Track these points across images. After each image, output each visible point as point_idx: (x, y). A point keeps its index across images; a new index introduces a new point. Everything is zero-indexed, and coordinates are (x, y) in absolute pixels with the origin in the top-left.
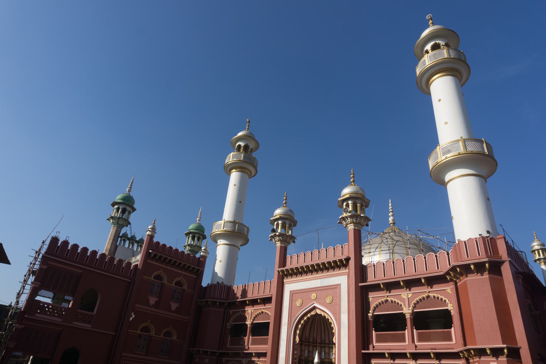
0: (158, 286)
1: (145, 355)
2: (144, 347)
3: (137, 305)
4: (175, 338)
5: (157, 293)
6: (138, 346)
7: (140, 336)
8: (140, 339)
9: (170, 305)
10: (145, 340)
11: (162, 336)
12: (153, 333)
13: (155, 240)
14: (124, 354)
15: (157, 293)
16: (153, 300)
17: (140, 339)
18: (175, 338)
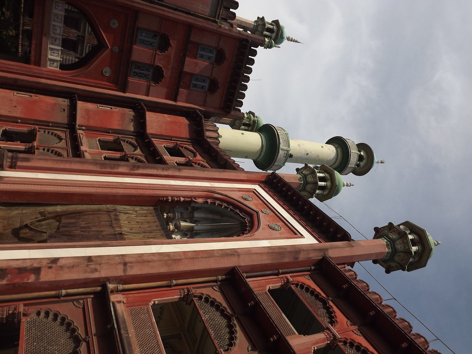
13: (260, 50)
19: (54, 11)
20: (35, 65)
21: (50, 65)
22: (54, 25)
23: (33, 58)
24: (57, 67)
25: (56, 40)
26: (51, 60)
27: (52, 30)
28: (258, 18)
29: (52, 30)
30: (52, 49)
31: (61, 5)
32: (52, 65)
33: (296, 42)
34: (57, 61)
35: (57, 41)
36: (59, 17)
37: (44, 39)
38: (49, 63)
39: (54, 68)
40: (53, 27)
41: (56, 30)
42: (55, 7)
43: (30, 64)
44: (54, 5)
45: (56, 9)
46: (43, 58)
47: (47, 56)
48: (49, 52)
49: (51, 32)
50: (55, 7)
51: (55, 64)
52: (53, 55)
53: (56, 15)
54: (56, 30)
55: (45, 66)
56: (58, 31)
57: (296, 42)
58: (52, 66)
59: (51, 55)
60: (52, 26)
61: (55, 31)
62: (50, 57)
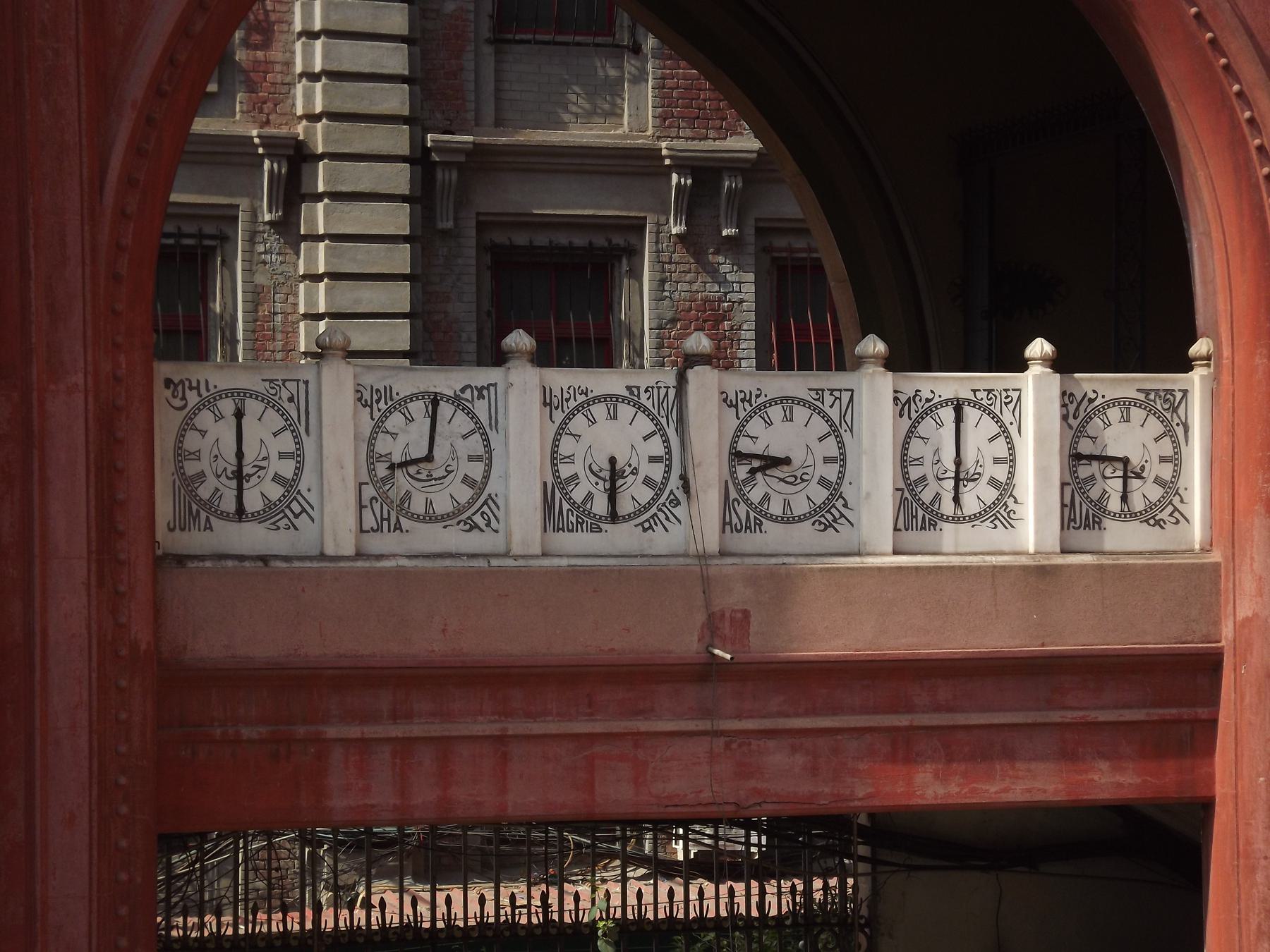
19: (336, 523)
20: (1200, 738)
21: (1150, 517)
22: (556, 507)
23: (1109, 780)
24: (1168, 409)
25: (771, 463)
26: (1079, 513)
27: (622, 538)
29: (622, 538)
30: (915, 512)
32: (1144, 493)
34: (1076, 416)
36: (407, 437)
37: (829, 633)
38: (1122, 538)
39: (1177, 434)
40: (586, 519)
41: (615, 475)
42: (271, 513)
43: (1207, 805)
44: (252, 538)
45: (287, 507)
46: (1079, 632)
47: (1039, 576)
48: (959, 544)
49: (666, 540)
50: (271, 513)
51: (1127, 437)
52: (1005, 489)
54: (615, 475)
55: (1200, 582)
56: (623, 437)
58: (1171, 488)
59: (999, 511)
60: (580, 542)
61: (634, 493)
62: (1032, 529)
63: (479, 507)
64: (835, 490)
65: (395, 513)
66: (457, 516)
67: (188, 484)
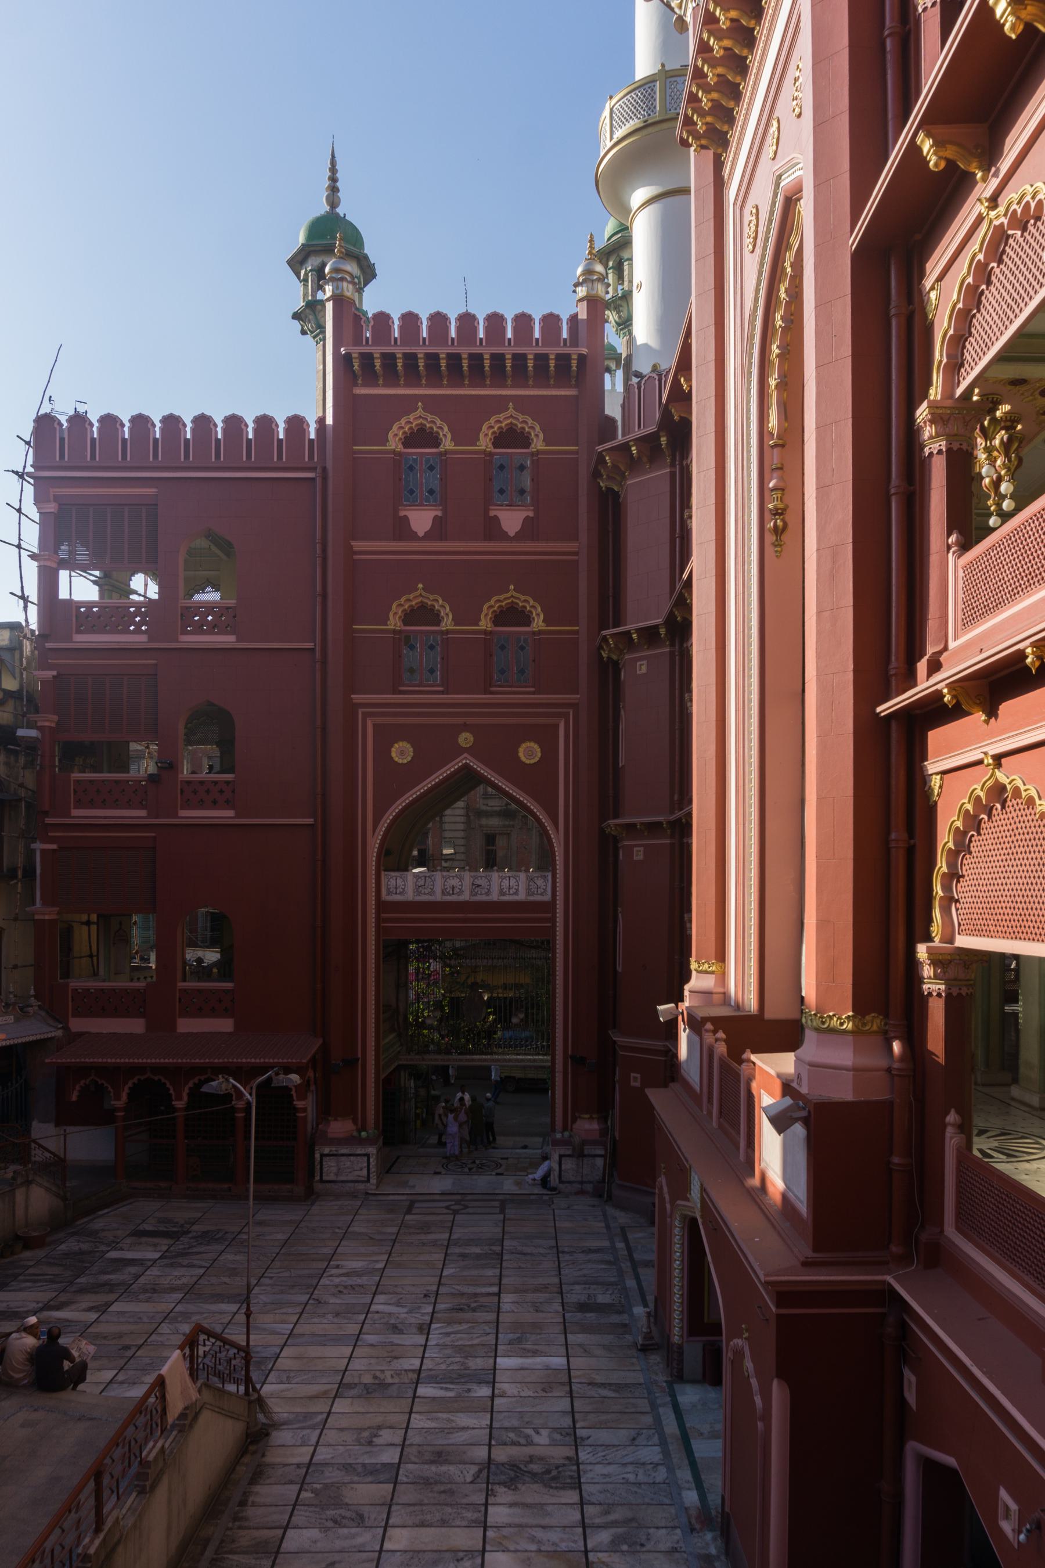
0: (431, 468)
1: (442, 693)
2: (432, 671)
3: (358, 545)
4: (538, 623)
5: (431, 492)
6: (412, 671)
7: (407, 638)
8: (412, 647)
9: (496, 518)
10: (432, 647)
11: (485, 623)
12: (447, 623)
14: (357, 698)
15: (431, 492)
16: (421, 520)
17: (412, 647)
18: (538, 623)
21: (542, 894)
22: (444, 892)
25: (479, 886)
28: (304, 332)
31: (393, 882)
33: (333, 169)
35: (479, 882)
41: (453, 888)
42: (400, 893)
50: (400, 893)
52: (517, 890)
53: (418, 889)
54: (453, 888)
57: (333, 169)
58: (545, 890)
59: (516, 893)
61: (457, 890)
63: (432, 892)
64: (489, 890)
65: (419, 893)
66: (429, 894)
67: (388, 889)
